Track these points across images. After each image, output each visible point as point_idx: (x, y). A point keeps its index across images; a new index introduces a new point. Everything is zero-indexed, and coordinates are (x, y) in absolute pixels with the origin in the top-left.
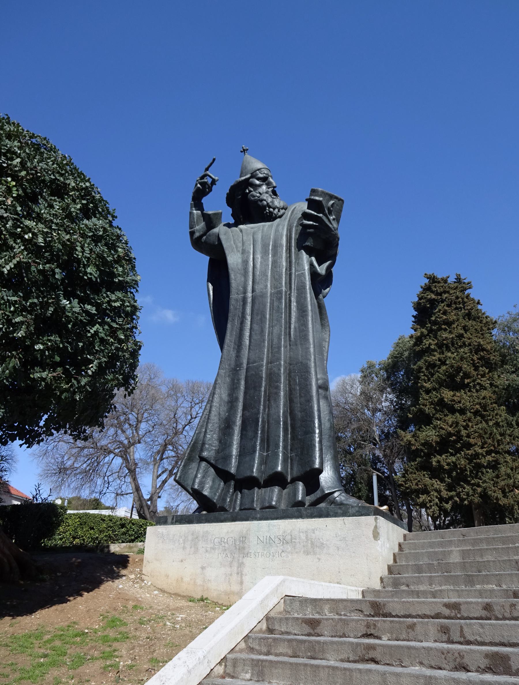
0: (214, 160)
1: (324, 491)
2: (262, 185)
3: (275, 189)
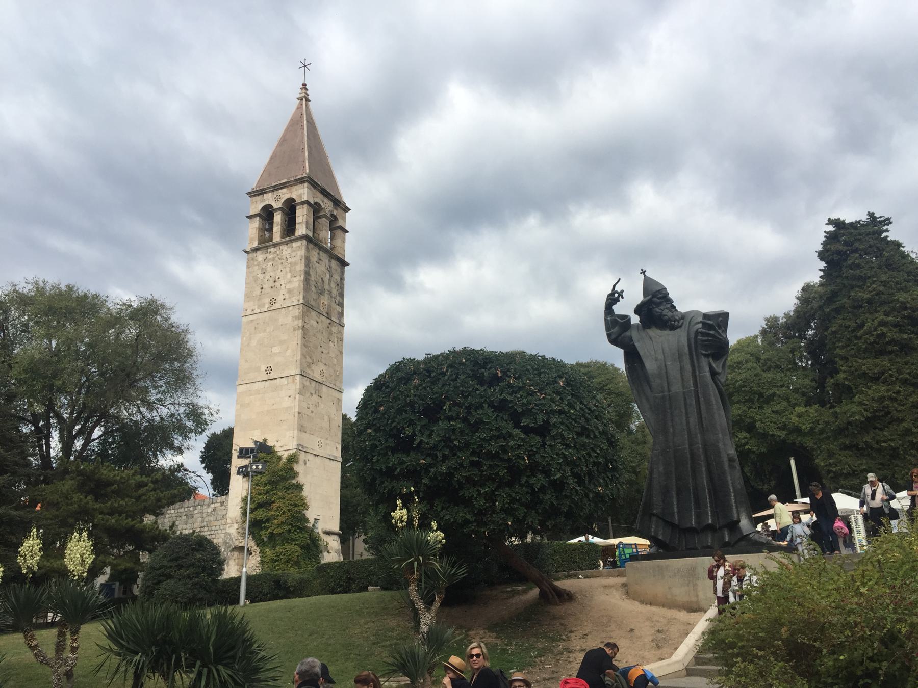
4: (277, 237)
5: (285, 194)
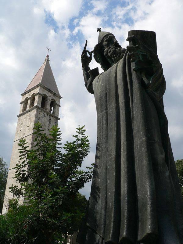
0: (87, 41)
4: (28, 108)
5: (32, 92)
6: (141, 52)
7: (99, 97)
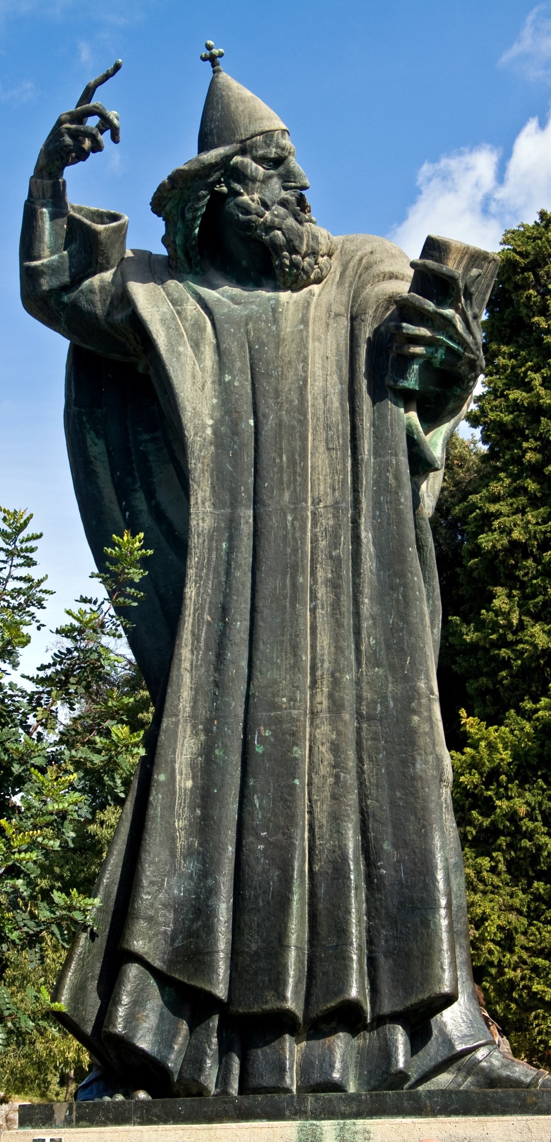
0: (117, 67)
1: (452, 1046)
2: (270, 177)
3: (303, 192)
6: (451, 338)
7: (209, 431)
